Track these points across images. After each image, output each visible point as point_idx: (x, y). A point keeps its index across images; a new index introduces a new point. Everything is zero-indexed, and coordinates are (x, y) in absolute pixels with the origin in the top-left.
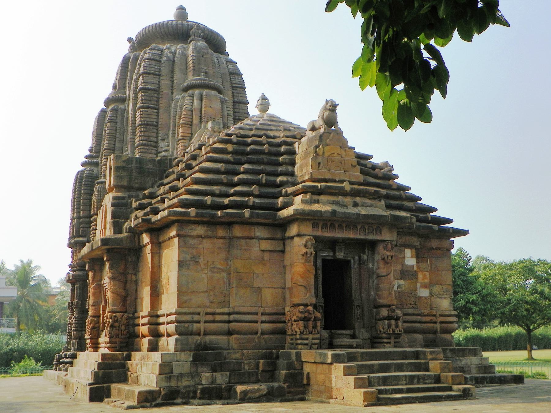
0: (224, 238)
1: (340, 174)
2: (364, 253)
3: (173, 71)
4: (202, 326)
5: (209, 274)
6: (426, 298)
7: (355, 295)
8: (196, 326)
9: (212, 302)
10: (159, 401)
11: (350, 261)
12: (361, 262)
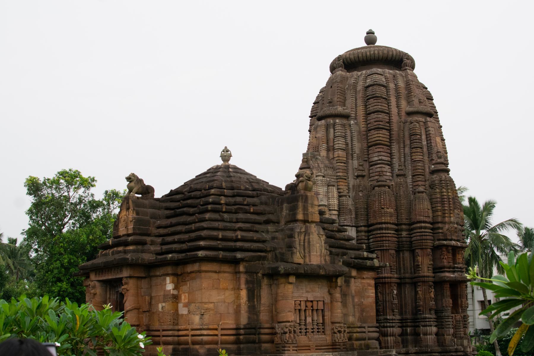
6: (186, 315)
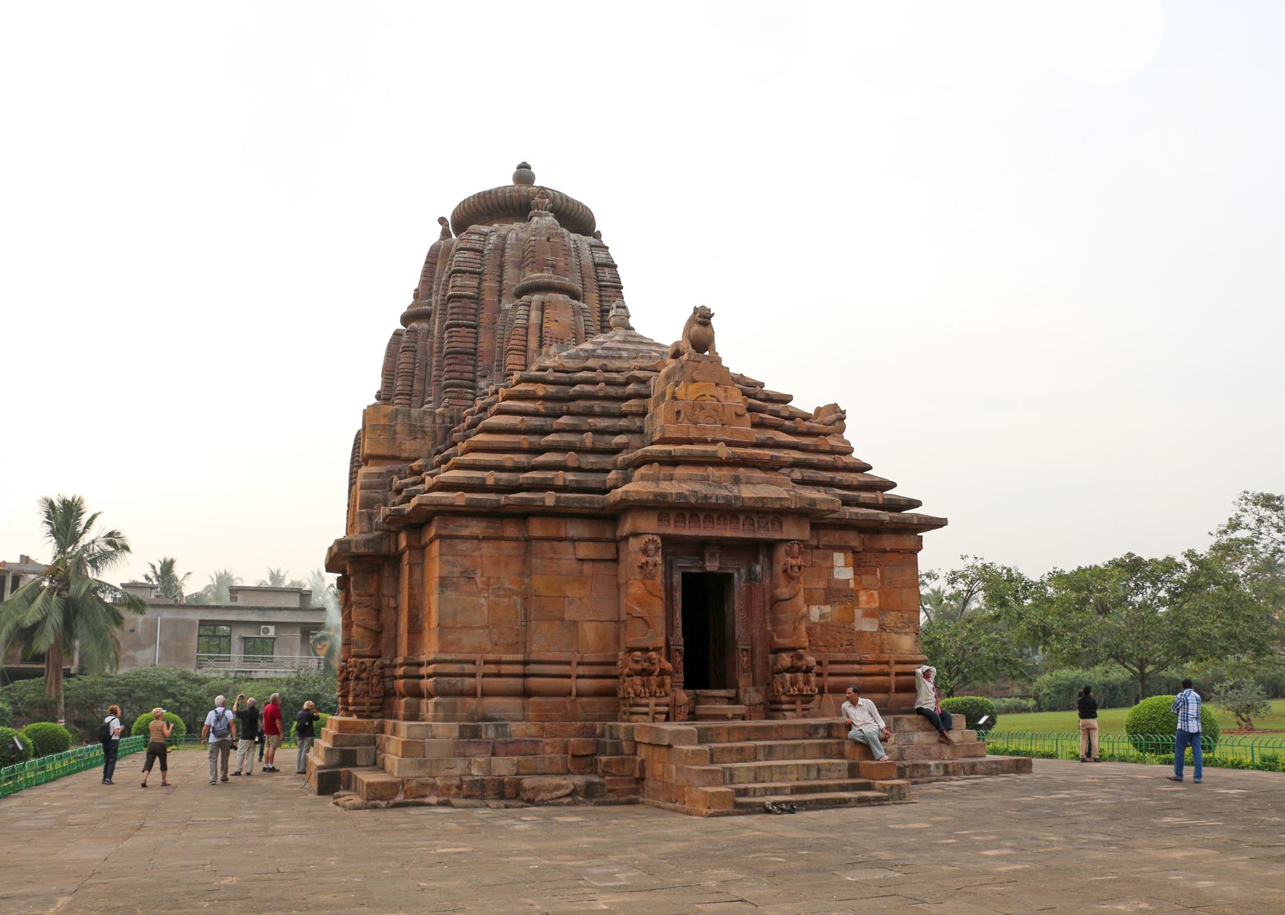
0: (516, 539)
1: (715, 429)
2: (757, 561)
3: (501, 266)
4: (478, 682)
5: (492, 598)
6: (872, 633)
7: (740, 631)
8: (468, 681)
9: (496, 644)
10: (400, 798)
11: (731, 575)
12: (751, 576)
